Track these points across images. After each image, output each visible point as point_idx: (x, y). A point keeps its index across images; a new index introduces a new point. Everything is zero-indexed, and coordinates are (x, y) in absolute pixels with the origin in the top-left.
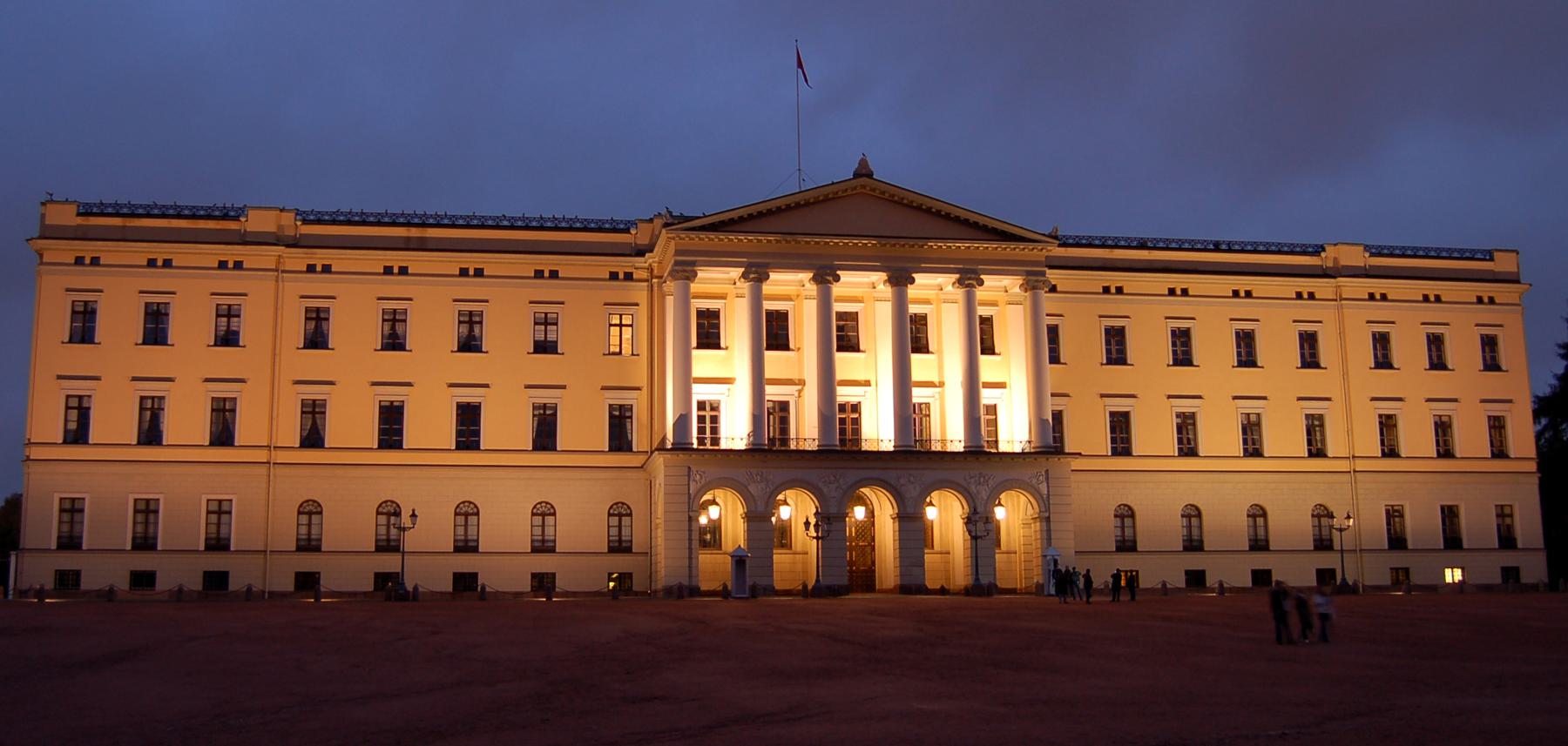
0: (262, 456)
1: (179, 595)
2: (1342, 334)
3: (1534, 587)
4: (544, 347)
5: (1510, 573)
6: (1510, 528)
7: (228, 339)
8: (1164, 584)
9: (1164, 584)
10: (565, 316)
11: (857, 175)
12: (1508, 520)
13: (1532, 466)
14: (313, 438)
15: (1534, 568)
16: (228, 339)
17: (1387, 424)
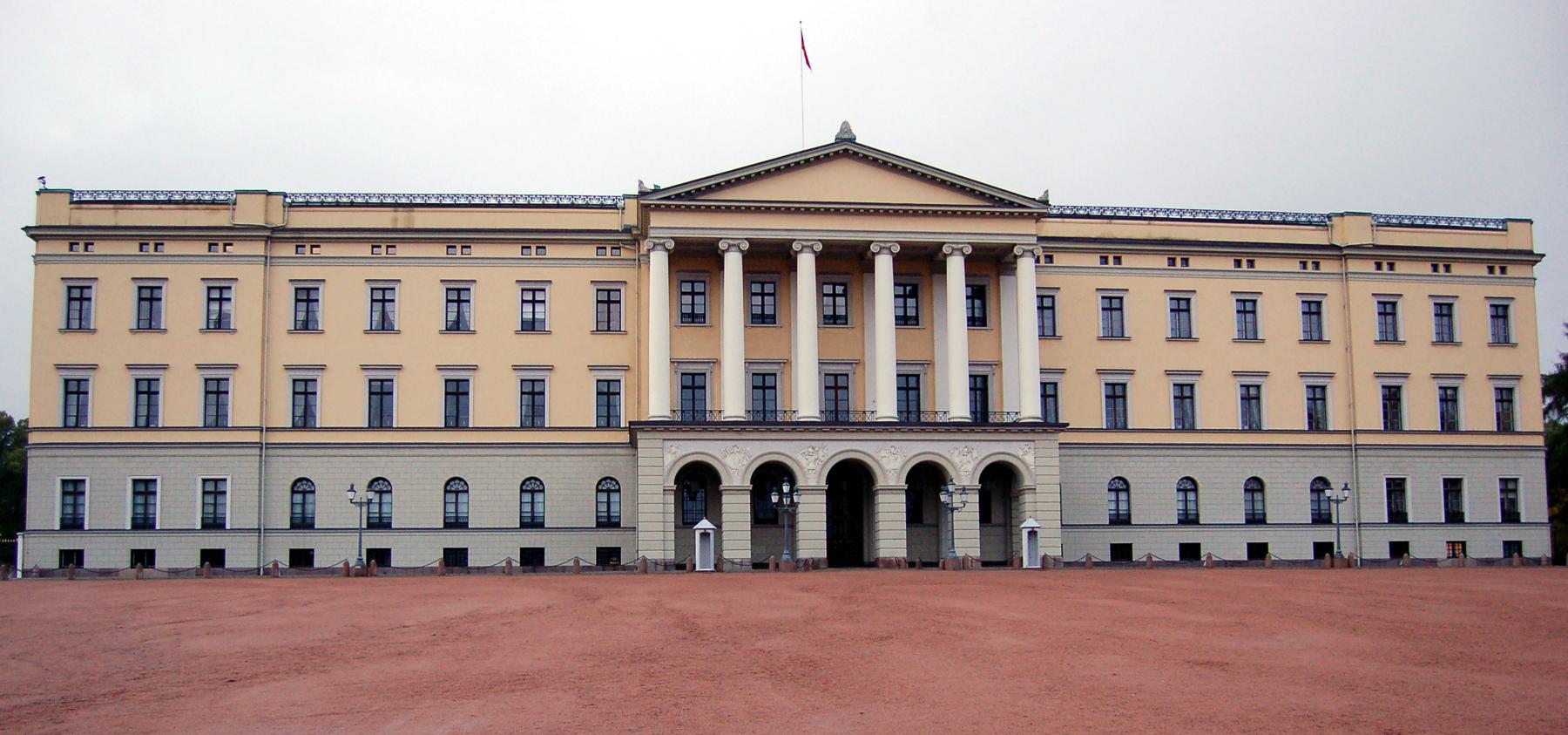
0: (254, 437)
1: (175, 573)
2: (1346, 306)
3: (1537, 562)
4: (530, 326)
5: (1512, 548)
6: (1514, 502)
7: (219, 324)
8: (1150, 557)
9: (1150, 557)
10: (550, 294)
12: (1511, 496)
13: (1539, 441)
14: (305, 419)
15: (1538, 543)
16: (219, 324)
17: (1392, 398)
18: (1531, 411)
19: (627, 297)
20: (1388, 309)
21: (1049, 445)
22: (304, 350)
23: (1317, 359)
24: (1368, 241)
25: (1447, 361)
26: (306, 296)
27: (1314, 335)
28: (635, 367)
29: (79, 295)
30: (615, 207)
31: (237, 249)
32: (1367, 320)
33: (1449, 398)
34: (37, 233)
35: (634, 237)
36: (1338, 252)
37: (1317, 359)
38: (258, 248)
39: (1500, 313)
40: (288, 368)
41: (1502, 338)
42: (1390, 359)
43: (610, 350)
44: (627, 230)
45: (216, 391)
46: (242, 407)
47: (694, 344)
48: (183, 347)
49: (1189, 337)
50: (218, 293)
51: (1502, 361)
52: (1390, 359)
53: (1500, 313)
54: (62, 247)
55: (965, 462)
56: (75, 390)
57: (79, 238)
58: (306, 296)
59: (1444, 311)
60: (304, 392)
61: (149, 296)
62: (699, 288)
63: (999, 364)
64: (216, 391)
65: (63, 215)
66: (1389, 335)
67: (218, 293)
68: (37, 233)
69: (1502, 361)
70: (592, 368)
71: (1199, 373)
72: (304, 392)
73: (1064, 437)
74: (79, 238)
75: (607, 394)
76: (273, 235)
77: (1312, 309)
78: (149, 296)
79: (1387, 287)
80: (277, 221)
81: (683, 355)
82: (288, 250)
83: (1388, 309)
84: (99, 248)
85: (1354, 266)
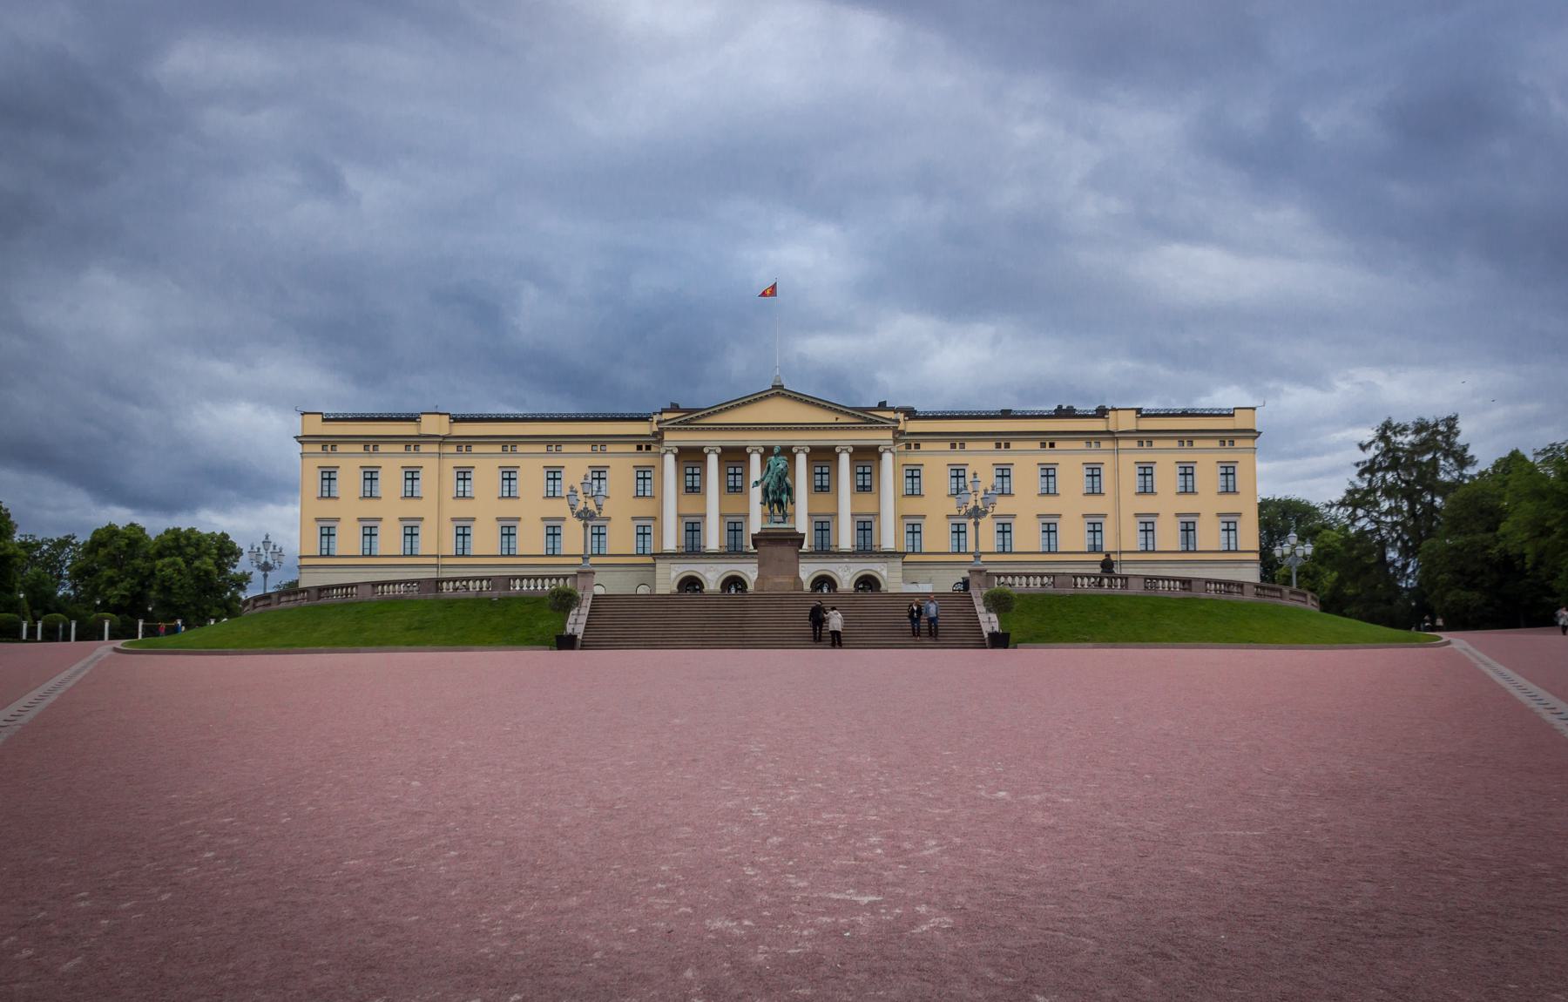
0: (434, 561)
11: (774, 387)
13: (1256, 557)
16: (411, 496)
18: (1249, 536)
19: (653, 474)
20: (1146, 471)
21: (898, 563)
22: (463, 509)
23: (1095, 505)
24: (1133, 427)
25: (1188, 504)
26: (464, 475)
27: (1094, 491)
28: (657, 518)
29: (328, 476)
30: (646, 420)
31: (423, 448)
32: (1131, 479)
33: (1188, 529)
34: (303, 440)
35: (658, 436)
36: (1111, 435)
37: (1095, 505)
38: (435, 448)
39: (1228, 471)
40: (453, 520)
41: (1229, 490)
42: (1146, 504)
43: (644, 508)
44: (655, 434)
45: (411, 533)
46: (426, 543)
47: (691, 505)
48: (391, 506)
49: (1010, 494)
50: (412, 475)
51: (1229, 504)
52: (1146, 504)
53: (1228, 471)
54: (318, 448)
55: (846, 575)
56: (328, 533)
57: (329, 443)
58: (464, 475)
59: (1187, 471)
60: (463, 533)
61: (370, 476)
62: (697, 471)
63: (878, 514)
64: (411, 533)
65: (317, 427)
66: (1146, 490)
67: (412, 475)
68: (303, 440)
69: (1229, 504)
70: (634, 519)
71: (1014, 516)
72: (463, 533)
73: (908, 558)
74: (329, 443)
75: (643, 534)
76: (443, 440)
77: (1094, 472)
78: (370, 476)
79: (1145, 457)
80: (444, 433)
81: (683, 512)
82: (453, 449)
83: (1146, 471)
84: (340, 448)
85: (1122, 444)
